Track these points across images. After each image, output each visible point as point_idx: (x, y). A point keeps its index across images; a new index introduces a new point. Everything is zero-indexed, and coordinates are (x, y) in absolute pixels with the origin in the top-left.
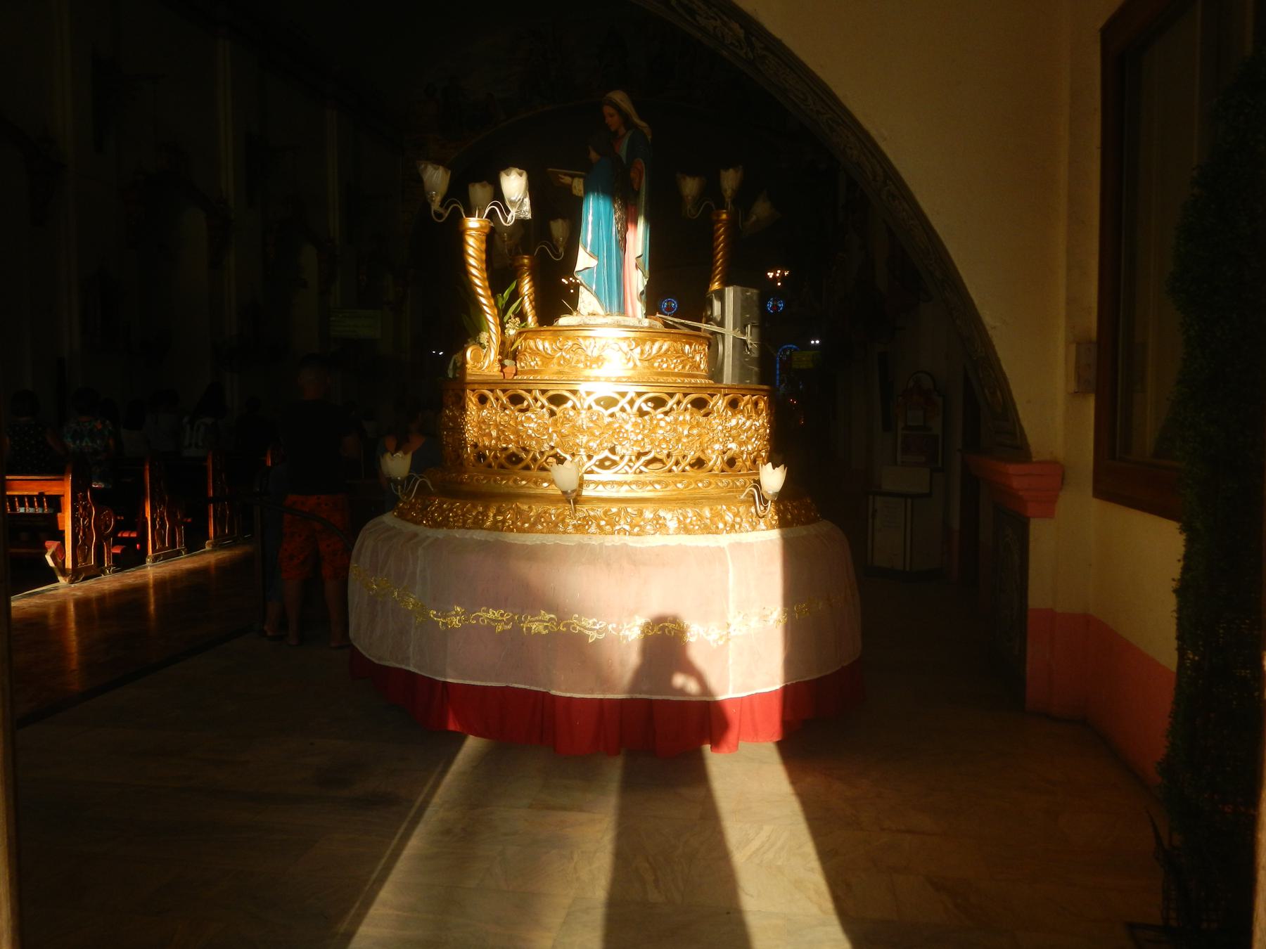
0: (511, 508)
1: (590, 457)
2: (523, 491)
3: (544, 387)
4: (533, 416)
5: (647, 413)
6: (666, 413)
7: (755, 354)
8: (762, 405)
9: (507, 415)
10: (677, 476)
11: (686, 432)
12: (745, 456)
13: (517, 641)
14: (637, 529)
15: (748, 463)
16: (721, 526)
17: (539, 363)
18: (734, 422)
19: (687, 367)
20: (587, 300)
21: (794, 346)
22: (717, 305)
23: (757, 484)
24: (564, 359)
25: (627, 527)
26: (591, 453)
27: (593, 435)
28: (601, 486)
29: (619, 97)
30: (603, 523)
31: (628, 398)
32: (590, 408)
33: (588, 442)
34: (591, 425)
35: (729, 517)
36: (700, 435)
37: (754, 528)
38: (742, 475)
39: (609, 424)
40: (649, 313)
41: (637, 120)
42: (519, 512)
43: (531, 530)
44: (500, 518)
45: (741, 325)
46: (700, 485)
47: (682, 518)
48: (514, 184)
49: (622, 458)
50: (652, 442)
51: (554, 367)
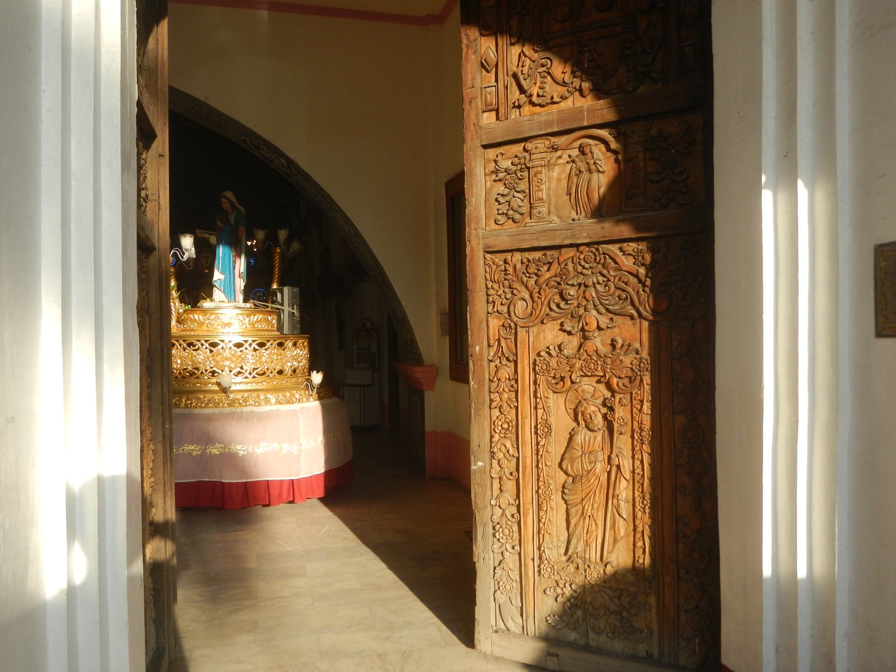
0: (195, 397)
1: (230, 371)
2: (198, 389)
3: (207, 339)
4: (201, 353)
5: (257, 350)
6: (266, 350)
7: (298, 319)
8: (306, 344)
9: (187, 352)
10: (271, 378)
11: (275, 358)
12: (300, 368)
13: (204, 460)
14: (257, 404)
15: (301, 371)
16: (294, 400)
17: (196, 326)
18: (295, 352)
19: (270, 327)
20: (217, 294)
21: (263, 290)
22: (279, 295)
23: (309, 381)
25: (253, 403)
26: (231, 369)
27: (232, 361)
28: (237, 384)
29: (229, 194)
30: (241, 401)
31: (249, 343)
32: (230, 348)
33: (230, 364)
34: (231, 356)
35: (297, 396)
36: (281, 359)
37: (308, 401)
38: (300, 377)
39: (240, 355)
41: (238, 205)
42: (199, 399)
44: (189, 402)
45: (292, 305)
46: (283, 382)
47: (277, 398)
48: (187, 242)
49: (246, 371)
50: (260, 363)
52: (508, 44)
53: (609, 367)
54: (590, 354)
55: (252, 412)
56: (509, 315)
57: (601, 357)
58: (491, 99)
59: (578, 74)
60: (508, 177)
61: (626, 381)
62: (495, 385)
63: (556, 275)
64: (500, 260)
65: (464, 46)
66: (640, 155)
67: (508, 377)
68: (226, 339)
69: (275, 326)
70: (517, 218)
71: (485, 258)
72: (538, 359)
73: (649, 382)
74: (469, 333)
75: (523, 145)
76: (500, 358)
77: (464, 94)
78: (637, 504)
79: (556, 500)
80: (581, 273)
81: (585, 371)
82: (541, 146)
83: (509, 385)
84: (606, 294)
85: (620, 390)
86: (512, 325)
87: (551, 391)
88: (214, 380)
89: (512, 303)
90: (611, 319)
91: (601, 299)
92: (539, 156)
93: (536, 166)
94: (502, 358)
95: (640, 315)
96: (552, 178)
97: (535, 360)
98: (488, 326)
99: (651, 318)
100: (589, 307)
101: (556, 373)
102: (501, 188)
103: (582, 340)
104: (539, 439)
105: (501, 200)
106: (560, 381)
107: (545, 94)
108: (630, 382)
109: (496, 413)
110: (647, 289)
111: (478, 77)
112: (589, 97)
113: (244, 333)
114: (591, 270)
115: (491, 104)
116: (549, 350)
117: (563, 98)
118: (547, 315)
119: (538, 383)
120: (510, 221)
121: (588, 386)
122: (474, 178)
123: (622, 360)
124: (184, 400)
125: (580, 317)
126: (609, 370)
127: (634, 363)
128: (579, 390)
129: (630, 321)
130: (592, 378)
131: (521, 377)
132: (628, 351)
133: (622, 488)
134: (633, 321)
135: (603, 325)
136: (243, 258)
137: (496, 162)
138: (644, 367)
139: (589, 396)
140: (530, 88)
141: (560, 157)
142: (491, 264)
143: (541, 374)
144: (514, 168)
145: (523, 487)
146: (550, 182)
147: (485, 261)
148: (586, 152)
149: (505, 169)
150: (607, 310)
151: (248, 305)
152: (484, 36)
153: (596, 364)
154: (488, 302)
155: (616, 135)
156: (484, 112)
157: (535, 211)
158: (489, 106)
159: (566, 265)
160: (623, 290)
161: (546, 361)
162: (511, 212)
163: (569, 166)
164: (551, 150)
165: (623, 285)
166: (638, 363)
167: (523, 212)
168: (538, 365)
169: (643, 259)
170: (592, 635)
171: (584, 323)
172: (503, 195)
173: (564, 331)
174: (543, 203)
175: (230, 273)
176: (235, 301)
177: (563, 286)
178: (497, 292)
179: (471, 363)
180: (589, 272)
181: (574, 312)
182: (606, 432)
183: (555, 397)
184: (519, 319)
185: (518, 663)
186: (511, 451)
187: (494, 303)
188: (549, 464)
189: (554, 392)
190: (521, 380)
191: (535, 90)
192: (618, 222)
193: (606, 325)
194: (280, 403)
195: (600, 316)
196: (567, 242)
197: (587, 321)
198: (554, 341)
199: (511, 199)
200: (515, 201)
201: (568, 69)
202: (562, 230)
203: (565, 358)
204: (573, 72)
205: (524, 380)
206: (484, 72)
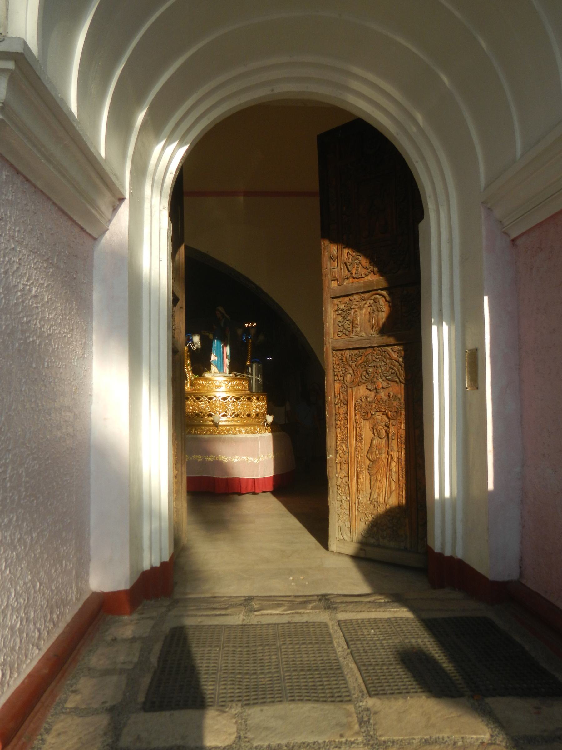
1: (220, 414)
3: (207, 395)
5: (235, 402)
6: (240, 402)
10: (243, 419)
11: (246, 407)
13: (204, 464)
16: (256, 432)
18: (258, 404)
20: (214, 369)
22: (250, 369)
23: (266, 421)
24: (209, 386)
25: (232, 432)
27: (221, 408)
28: (223, 421)
29: (220, 309)
32: (220, 400)
35: (258, 429)
36: (249, 407)
37: (265, 433)
39: (225, 405)
40: (230, 373)
41: (226, 315)
42: (201, 429)
43: (206, 434)
44: (196, 431)
45: (257, 375)
48: (196, 339)
49: (229, 414)
50: (237, 409)
51: (206, 388)
52: (342, 247)
53: (387, 406)
54: (379, 400)
55: (232, 438)
56: (344, 382)
58: (335, 274)
59: (372, 264)
61: (395, 414)
62: (338, 416)
65: (322, 248)
68: (217, 395)
69: (247, 387)
74: (326, 391)
75: (349, 297)
77: (323, 272)
78: (400, 474)
79: (365, 472)
80: (375, 361)
82: (357, 298)
86: (345, 386)
88: (211, 419)
90: (388, 383)
92: (356, 303)
95: (400, 381)
102: (340, 319)
104: (358, 443)
105: (340, 325)
107: (358, 273)
108: (397, 414)
109: (338, 430)
111: (329, 264)
112: (378, 275)
113: (228, 392)
115: (335, 277)
117: (367, 275)
120: (344, 335)
121: (379, 416)
124: (193, 430)
128: (375, 418)
133: (393, 466)
135: (384, 386)
136: (228, 347)
139: (379, 421)
141: (365, 304)
144: (346, 309)
145: (350, 468)
150: (386, 379)
151: (231, 375)
152: (332, 243)
154: (335, 375)
156: (332, 281)
157: (354, 330)
162: (344, 331)
163: (370, 308)
164: (361, 300)
167: (350, 330)
169: (401, 354)
170: (381, 540)
172: (341, 322)
173: (368, 389)
175: (220, 356)
176: (224, 373)
177: (367, 367)
179: (326, 405)
182: (387, 439)
183: (365, 422)
185: (347, 555)
186: (345, 449)
187: (337, 375)
188: (362, 455)
189: (364, 420)
191: (354, 271)
192: (389, 336)
194: (248, 433)
196: (368, 345)
200: (346, 325)
201: (368, 261)
204: (370, 263)
206: (332, 261)
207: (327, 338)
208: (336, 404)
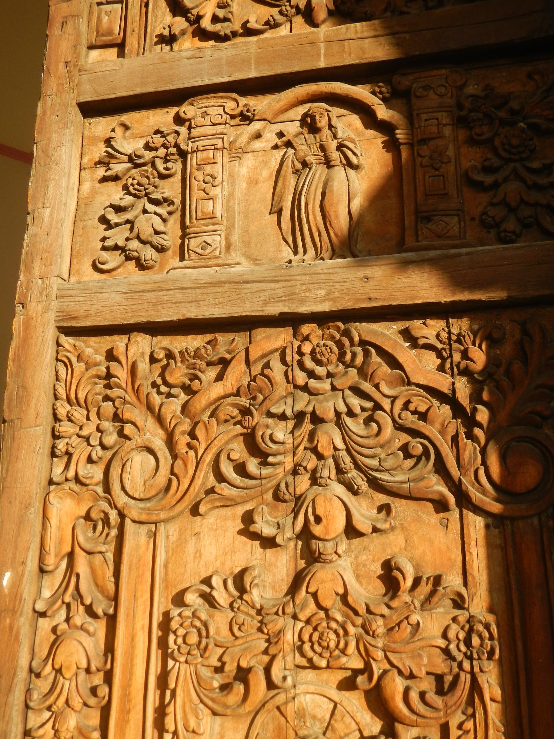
53: (380, 643)
54: (326, 603)
56: (107, 489)
57: (356, 613)
58: (110, 22)
60: (134, 171)
63: (238, 390)
64: (96, 352)
66: (447, 131)
67: (84, 665)
70: (148, 257)
71: (58, 345)
72: (175, 612)
73: (498, 693)
76: (68, 606)
80: (305, 388)
81: (310, 654)
83: (85, 691)
84: (370, 442)
85: (414, 717)
86: (113, 515)
87: (207, 711)
89: (118, 457)
91: (358, 457)
93: (202, 148)
94: (73, 607)
96: (239, 176)
97: (167, 617)
98: (45, 516)
99: (496, 508)
100: (325, 473)
101: (226, 658)
103: (302, 564)
105: (114, 218)
106: (236, 678)
107: (230, 16)
108: (440, 691)
110: (478, 431)
114: (329, 380)
115: (110, 32)
116: (208, 590)
117: (272, 25)
118: (212, 491)
119: (172, 685)
120: (132, 265)
122: (54, 166)
123: (418, 624)
125: (299, 500)
126: (380, 655)
127: (451, 634)
128: (290, 710)
129: (435, 515)
130: (325, 675)
131: (124, 666)
132: (435, 599)
134: (442, 515)
137: (108, 142)
138: (481, 645)
140: (197, 6)
141: (258, 136)
142: (74, 360)
143: (183, 659)
144: (148, 155)
146: (233, 183)
147: (57, 352)
148: (319, 125)
149: (130, 156)
153: (341, 632)
154: (53, 455)
155: (387, 95)
156: (91, 47)
157: (193, 243)
158: (103, 35)
159: (267, 365)
160: (415, 433)
161: (199, 618)
162: (134, 244)
163: (278, 155)
164: (237, 121)
165: (415, 418)
166: (462, 635)
168: (175, 632)
169: (465, 355)
171: (311, 517)
172: (118, 209)
173: (255, 536)
174: (215, 224)
177: (258, 418)
178: (81, 428)
180: (326, 385)
181: (283, 486)
183: (217, 728)
184: (133, 502)
187: (69, 455)
190: (123, 673)
193: (370, 523)
195: (353, 498)
196: (274, 309)
197: (319, 512)
198: (223, 564)
199: (136, 217)
202: (260, 282)
203: (253, 612)
205: (131, 679)
207: (37, 273)
208: (43, 615)
